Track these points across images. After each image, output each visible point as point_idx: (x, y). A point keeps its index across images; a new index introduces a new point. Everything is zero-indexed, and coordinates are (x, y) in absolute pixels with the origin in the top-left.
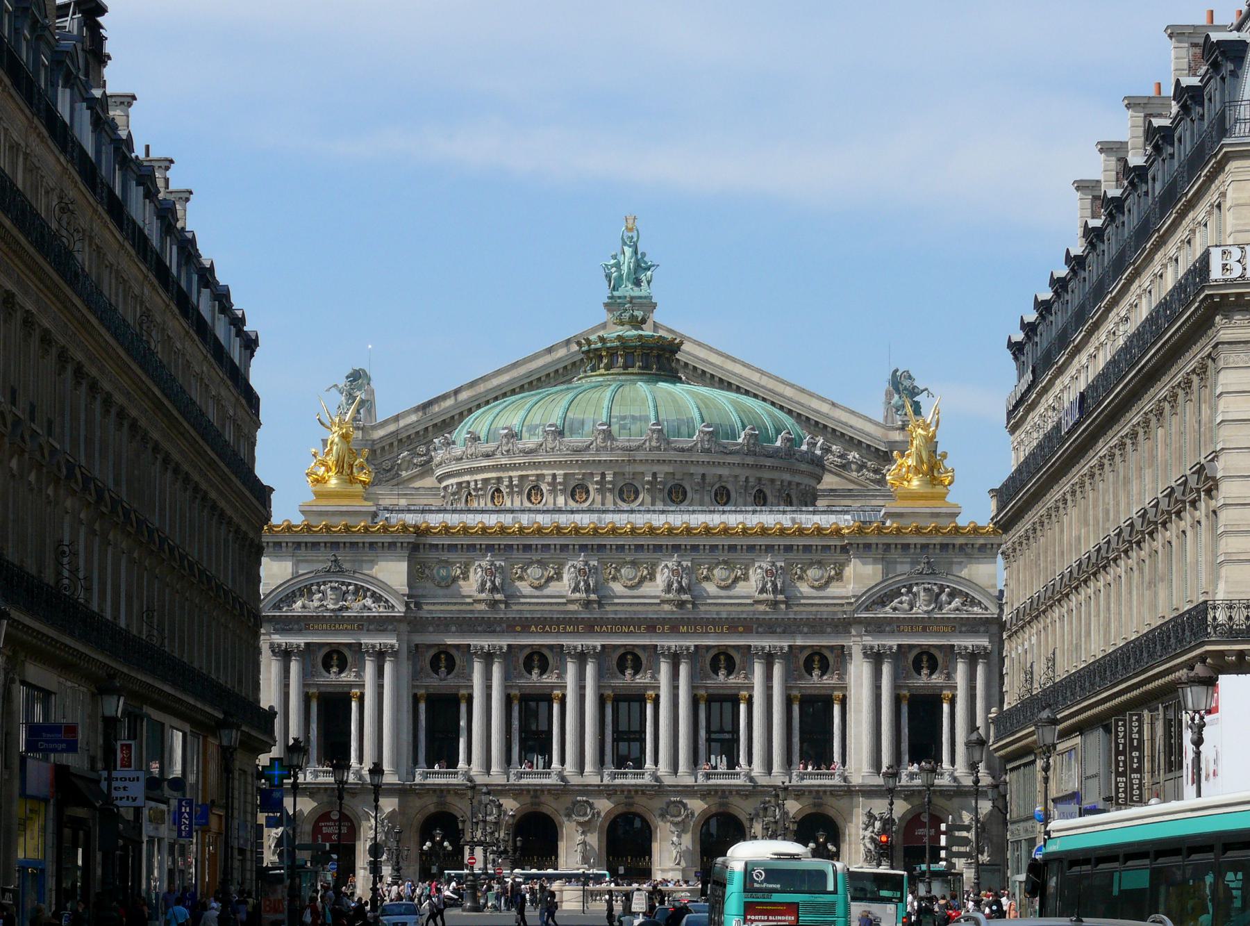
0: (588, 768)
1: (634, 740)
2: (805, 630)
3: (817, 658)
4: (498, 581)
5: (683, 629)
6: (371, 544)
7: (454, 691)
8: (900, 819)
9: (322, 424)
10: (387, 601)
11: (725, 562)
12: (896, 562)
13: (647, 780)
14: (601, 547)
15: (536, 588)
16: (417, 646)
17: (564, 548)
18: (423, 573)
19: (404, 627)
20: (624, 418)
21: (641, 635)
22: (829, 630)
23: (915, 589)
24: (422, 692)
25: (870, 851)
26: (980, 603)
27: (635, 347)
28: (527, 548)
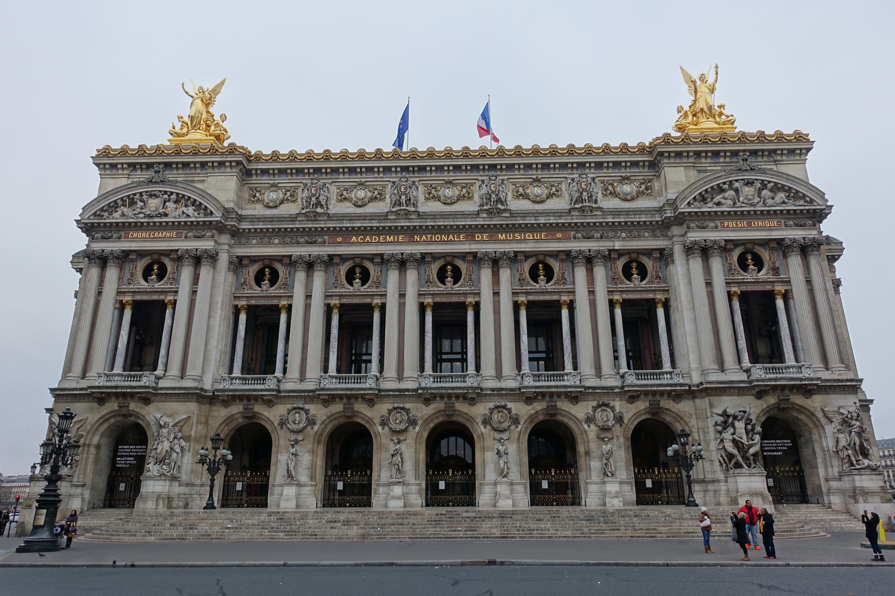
0: (406, 374)
2: (624, 235)
3: (634, 265)
4: (322, 199)
5: (501, 237)
6: (203, 165)
7: (275, 302)
9: (187, 93)
11: (537, 180)
12: (706, 171)
13: (470, 382)
14: (422, 169)
15: (360, 206)
16: (240, 259)
17: (387, 169)
18: (255, 196)
19: (225, 239)
22: (646, 234)
24: (242, 303)
25: (731, 456)
26: (804, 196)
28: (352, 170)
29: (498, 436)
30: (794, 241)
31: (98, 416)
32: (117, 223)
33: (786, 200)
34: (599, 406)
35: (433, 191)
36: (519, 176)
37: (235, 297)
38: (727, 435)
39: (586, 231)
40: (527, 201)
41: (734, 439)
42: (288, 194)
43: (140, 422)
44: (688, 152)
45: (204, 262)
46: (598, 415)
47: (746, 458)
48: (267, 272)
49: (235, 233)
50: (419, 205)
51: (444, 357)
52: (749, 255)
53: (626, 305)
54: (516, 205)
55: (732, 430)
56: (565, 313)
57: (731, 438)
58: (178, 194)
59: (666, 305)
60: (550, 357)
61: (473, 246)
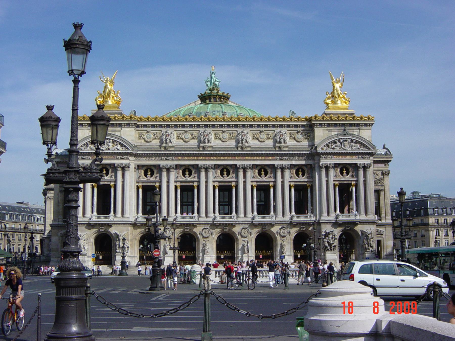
0: (209, 215)
1: (226, 205)
4: (171, 139)
6: (120, 125)
8: (338, 234)
10: (125, 146)
12: (332, 131)
14: (213, 126)
16: (138, 166)
20: (214, 111)
21: (230, 160)
23: (341, 141)
24: (140, 184)
25: (326, 247)
26: (367, 146)
27: (216, 96)
28: (183, 126)
29: (244, 239)
30: (360, 164)
31: (93, 232)
32: (89, 153)
33: (359, 147)
34: (282, 228)
35: (218, 135)
36: (255, 130)
37: (137, 182)
38: (326, 240)
39: (281, 156)
40: (258, 141)
41: (328, 242)
42: (156, 135)
43: (108, 233)
44: (324, 124)
45: (127, 169)
46: (282, 231)
47: (331, 248)
48: (149, 170)
49: (136, 155)
50: (212, 142)
51: (221, 203)
52: (344, 168)
53: (296, 187)
54: (252, 142)
55: (327, 238)
56: (272, 190)
57: (326, 240)
58: (112, 140)
59: (312, 187)
60: (264, 208)
61: (235, 162)
